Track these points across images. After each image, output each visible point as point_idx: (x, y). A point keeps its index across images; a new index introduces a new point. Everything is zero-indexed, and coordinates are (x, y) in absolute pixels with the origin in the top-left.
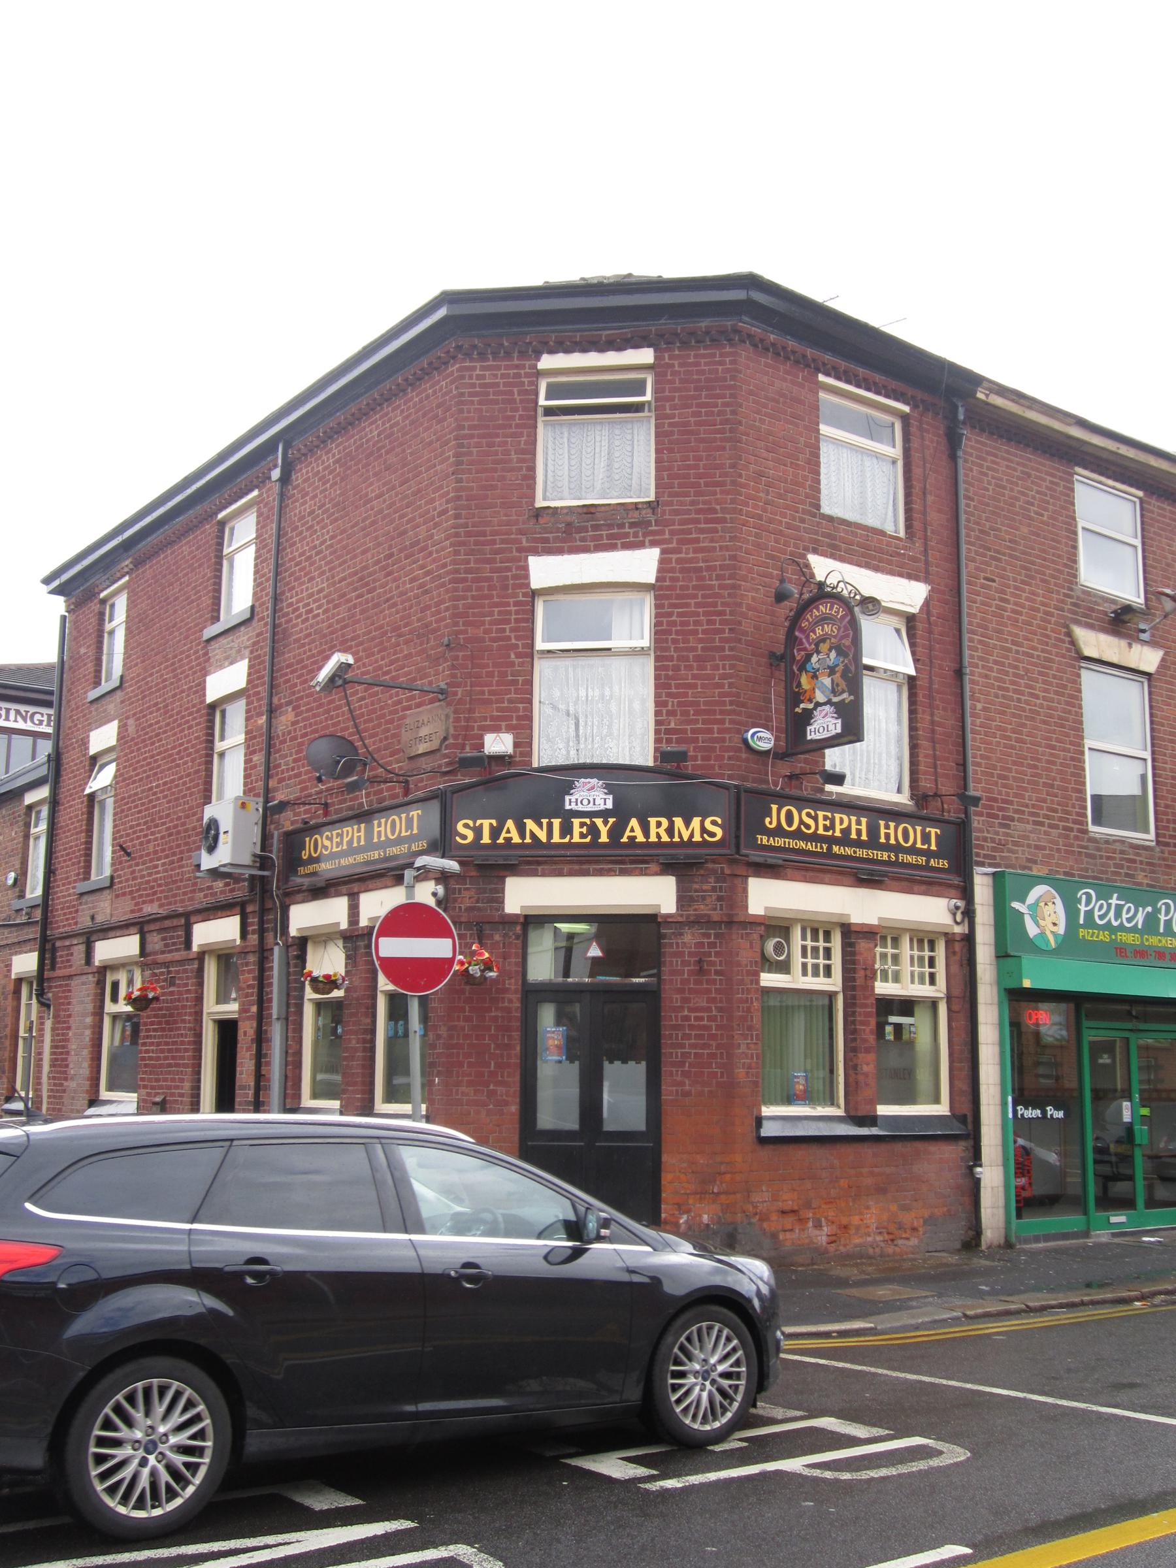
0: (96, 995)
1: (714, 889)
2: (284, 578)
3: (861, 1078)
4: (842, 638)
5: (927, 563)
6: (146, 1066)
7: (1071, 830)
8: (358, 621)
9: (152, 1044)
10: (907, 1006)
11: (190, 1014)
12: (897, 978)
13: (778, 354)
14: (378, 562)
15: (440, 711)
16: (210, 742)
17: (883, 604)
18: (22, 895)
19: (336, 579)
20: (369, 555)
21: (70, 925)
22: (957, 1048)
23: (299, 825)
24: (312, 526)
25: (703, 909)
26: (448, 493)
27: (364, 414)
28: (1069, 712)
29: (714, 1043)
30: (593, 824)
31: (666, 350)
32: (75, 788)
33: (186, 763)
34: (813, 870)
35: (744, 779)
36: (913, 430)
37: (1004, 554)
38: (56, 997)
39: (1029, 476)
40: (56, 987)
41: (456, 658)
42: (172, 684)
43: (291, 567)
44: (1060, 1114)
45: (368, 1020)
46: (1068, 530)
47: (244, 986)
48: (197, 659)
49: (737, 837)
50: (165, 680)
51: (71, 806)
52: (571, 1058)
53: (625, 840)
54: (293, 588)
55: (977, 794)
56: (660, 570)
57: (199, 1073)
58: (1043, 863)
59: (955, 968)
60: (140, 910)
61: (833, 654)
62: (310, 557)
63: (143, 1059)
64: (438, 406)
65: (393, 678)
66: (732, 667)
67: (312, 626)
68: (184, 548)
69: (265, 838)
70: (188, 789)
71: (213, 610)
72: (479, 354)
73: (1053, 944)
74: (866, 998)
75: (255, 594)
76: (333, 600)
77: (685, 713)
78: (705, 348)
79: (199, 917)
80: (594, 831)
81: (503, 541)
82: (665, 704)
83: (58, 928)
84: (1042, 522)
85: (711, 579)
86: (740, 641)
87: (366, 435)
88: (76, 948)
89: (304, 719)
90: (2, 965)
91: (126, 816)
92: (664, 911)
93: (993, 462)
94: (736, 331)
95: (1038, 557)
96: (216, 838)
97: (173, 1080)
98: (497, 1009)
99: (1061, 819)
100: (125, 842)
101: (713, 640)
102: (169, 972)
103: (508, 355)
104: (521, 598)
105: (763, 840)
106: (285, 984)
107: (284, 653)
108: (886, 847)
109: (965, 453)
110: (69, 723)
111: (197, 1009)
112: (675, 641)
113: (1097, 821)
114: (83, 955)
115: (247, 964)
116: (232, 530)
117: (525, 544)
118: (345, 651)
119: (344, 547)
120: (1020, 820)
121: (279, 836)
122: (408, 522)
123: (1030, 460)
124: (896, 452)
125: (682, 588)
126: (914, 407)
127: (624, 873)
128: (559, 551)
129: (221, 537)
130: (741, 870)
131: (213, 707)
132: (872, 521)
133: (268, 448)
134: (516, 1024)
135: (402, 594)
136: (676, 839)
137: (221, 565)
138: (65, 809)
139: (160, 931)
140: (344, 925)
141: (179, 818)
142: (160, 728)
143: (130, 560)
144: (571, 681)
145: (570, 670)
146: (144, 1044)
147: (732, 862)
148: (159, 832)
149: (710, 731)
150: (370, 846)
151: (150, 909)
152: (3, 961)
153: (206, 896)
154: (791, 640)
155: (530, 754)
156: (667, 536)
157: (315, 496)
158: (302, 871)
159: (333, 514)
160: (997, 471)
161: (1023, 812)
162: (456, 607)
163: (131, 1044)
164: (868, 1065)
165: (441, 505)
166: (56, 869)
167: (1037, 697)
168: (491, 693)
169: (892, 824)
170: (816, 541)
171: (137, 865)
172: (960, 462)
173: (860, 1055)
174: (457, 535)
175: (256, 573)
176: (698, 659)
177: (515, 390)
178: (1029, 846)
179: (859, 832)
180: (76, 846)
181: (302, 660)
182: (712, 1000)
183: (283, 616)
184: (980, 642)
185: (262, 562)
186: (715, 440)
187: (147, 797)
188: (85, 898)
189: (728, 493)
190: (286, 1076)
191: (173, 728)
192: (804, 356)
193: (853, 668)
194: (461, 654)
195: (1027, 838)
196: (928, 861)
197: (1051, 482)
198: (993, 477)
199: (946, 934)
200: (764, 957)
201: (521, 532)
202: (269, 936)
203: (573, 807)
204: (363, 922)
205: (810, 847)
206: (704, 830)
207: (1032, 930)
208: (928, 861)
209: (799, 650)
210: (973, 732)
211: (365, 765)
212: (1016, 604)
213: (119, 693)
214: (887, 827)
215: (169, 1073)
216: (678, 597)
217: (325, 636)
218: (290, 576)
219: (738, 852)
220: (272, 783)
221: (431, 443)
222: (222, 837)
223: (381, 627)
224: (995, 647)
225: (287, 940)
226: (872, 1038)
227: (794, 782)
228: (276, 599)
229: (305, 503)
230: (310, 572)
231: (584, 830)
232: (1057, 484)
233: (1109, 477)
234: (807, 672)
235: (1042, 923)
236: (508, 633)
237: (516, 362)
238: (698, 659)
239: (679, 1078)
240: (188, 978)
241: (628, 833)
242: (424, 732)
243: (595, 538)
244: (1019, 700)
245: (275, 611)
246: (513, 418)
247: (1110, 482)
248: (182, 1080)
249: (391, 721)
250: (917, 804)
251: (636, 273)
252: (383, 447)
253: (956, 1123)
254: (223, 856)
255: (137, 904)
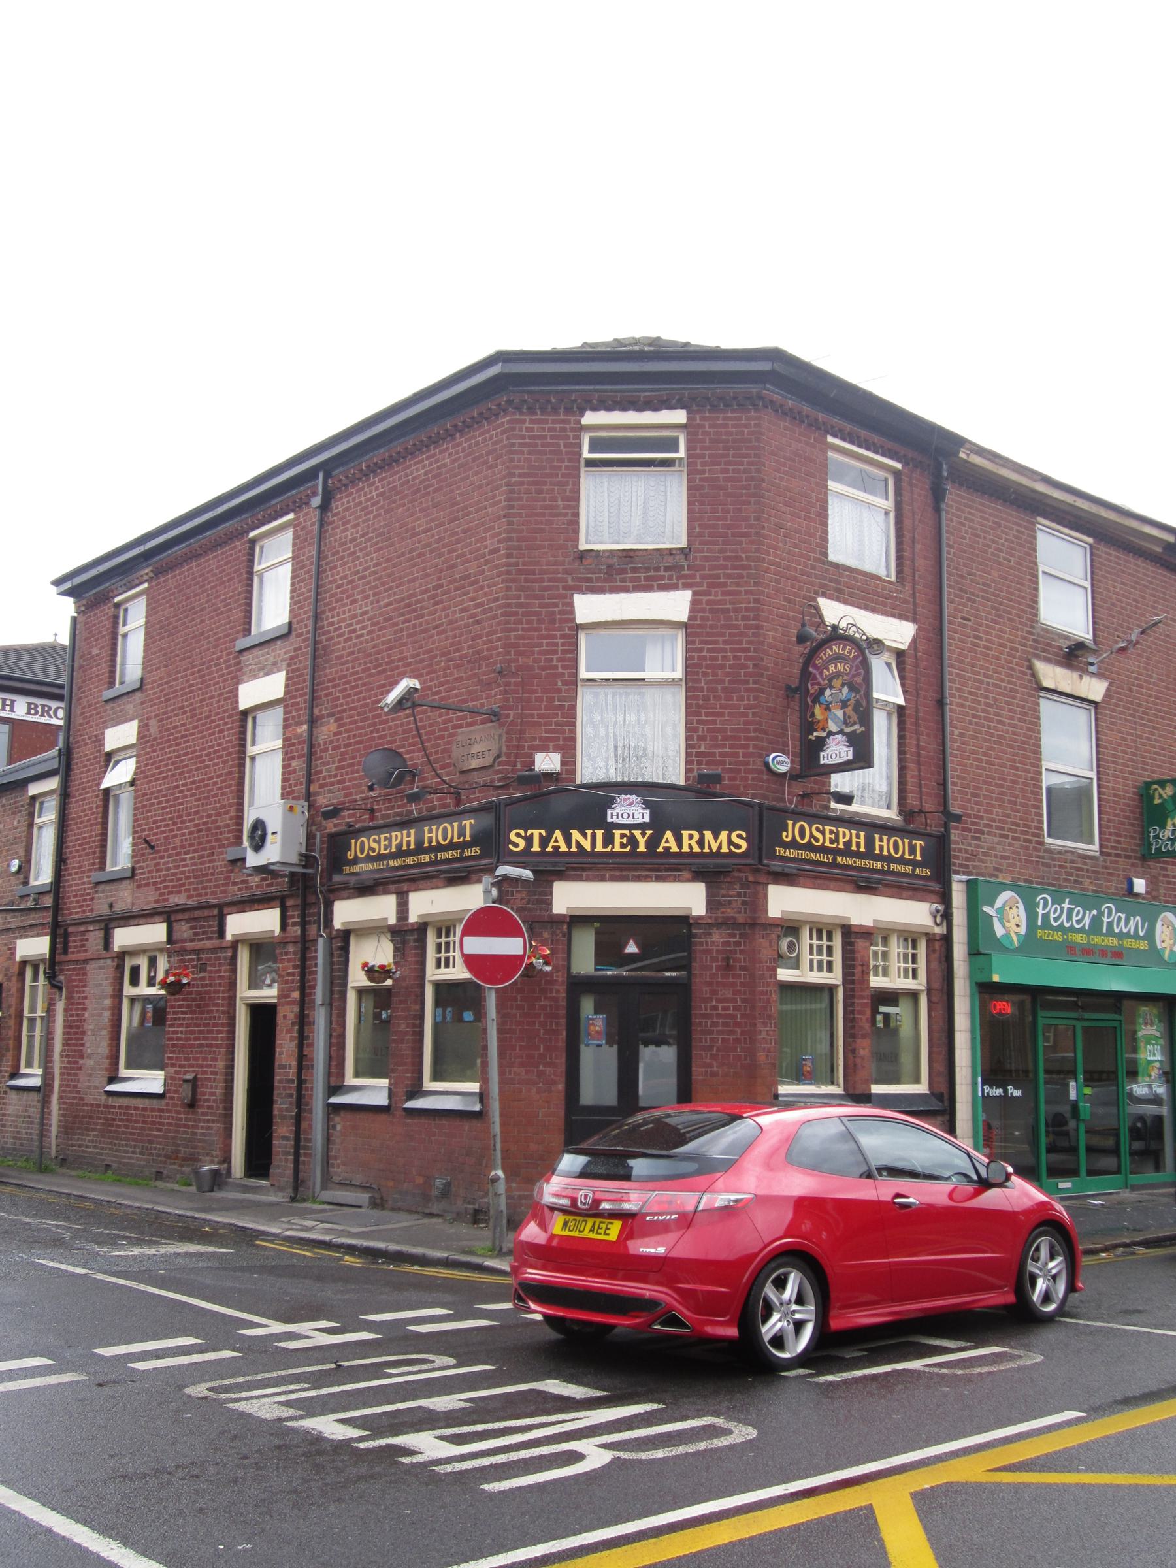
0: (115, 978)
1: (739, 895)
2: (325, 598)
3: (858, 1061)
4: (854, 676)
5: (915, 604)
6: (173, 1045)
7: (1030, 841)
8: (405, 644)
9: (180, 1025)
10: (890, 997)
11: (224, 998)
12: (886, 974)
13: (795, 418)
14: (427, 591)
15: (493, 731)
16: (243, 746)
17: (887, 643)
18: (26, 882)
19: (382, 603)
20: (417, 584)
21: (84, 912)
22: (935, 1034)
23: (343, 828)
24: (354, 553)
25: (729, 912)
26: (499, 534)
27: (409, 453)
28: (1030, 737)
29: (739, 1030)
30: (633, 835)
31: (698, 412)
32: (88, 782)
33: (215, 765)
34: (821, 878)
35: (765, 797)
36: (904, 485)
37: (978, 596)
38: (69, 980)
39: (999, 525)
40: (68, 970)
41: (508, 684)
42: (199, 689)
43: (331, 589)
44: (1018, 1093)
45: (418, 1007)
46: (1031, 574)
47: (284, 973)
48: (227, 667)
49: (760, 849)
50: (192, 685)
51: (84, 799)
52: (610, 1043)
53: (660, 850)
54: (335, 608)
55: (959, 812)
56: (692, 611)
57: (233, 1053)
58: (1007, 871)
59: (934, 965)
60: (167, 900)
61: (845, 690)
62: (353, 581)
63: (170, 1039)
64: (488, 453)
65: (442, 699)
66: (755, 698)
67: (355, 645)
68: (212, 562)
69: (310, 837)
70: (219, 789)
71: (245, 623)
72: (529, 408)
73: (1016, 943)
74: (863, 990)
75: (291, 611)
76: (378, 623)
77: (714, 739)
78: (733, 411)
79: (234, 909)
80: (633, 841)
81: (550, 580)
82: (695, 730)
83: (71, 914)
84: (1010, 567)
85: (737, 620)
86: (762, 675)
87: (412, 473)
88: (92, 934)
89: (347, 731)
90: (5, 948)
91: (149, 811)
92: (695, 913)
93: (970, 513)
94: (760, 397)
95: (1006, 598)
96: (263, 838)
97: (205, 1059)
98: (546, 998)
99: (1022, 832)
100: (148, 835)
101: (739, 674)
102: (199, 959)
103: (555, 410)
104: (567, 632)
105: (781, 851)
106: (328, 970)
107: (325, 669)
108: (880, 858)
109: (948, 505)
110: (80, 720)
111: (231, 993)
112: (704, 674)
113: (1049, 836)
114: (102, 942)
115: (286, 954)
116: (262, 548)
117: (570, 583)
118: (415, 677)
119: (390, 575)
120: (989, 833)
121: (322, 836)
122: (458, 557)
123: (1000, 511)
124: (890, 504)
125: (711, 627)
126: (905, 464)
127: (659, 879)
128: (601, 590)
129: (252, 554)
130: (762, 878)
131: (245, 713)
132: (868, 567)
133: (311, 474)
134: (563, 1012)
135: (451, 623)
136: (706, 850)
137: (252, 580)
138: (77, 801)
139: (188, 920)
140: (392, 920)
141: (209, 816)
142: (186, 730)
143: (150, 568)
144: (611, 707)
145: (610, 697)
146: (172, 1026)
147: (756, 871)
148: (187, 828)
149: (737, 755)
150: (420, 849)
151: (176, 900)
152: (5, 944)
153: (240, 889)
154: (805, 675)
155: (574, 772)
156: (698, 580)
157: (358, 525)
158: (346, 869)
159: (377, 543)
160: (972, 521)
161: (991, 826)
162: (508, 638)
163: (154, 1023)
164: (864, 1049)
165: (492, 544)
166: (67, 858)
167: (1003, 724)
168: (540, 716)
169: (885, 838)
170: (824, 586)
171: (162, 857)
172: (944, 514)
173: (859, 1041)
174: (508, 572)
175: (292, 591)
176: (725, 690)
177: (562, 442)
178: (996, 856)
179: (858, 844)
180: (91, 837)
181: (345, 676)
182: (736, 992)
183: (324, 634)
184: (958, 675)
185: (299, 582)
186: (741, 495)
187: (173, 794)
188: (102, 887)
189: (752, 542)
190: (330, 1057)
191: (202, 732)
192: (816, 420)
193: (864, 704)
194: (513, 680)
195: (994, 849)
196: (914, 870)
197: (1018, 531)
198: (970, 527)
199: (927, 934)
200: (780, 956)
201: (566, 572)
202: (312, 930)
203: (615, 820)
204: (413, 918)
205: (819, 857)
206: (730, 842)
207: (999, 931)
208: (914, 870)
209: (813, 684)
210: (952, 755)
211: (414, 776)
212: (987, 640)
213: (138, 694)
214: (881, 840)
215: (201, 1052)
216: (708, 634)
217: (369, 655)
218: (331, 597)
219: (760, 861)
220: (314, 788)
221: (480, 487)
222: (269, 838)
223: (431, 651)
224: (970, 679)
225: (331, 933)
226: (867, 1026)
227: (806, 800)
228: (317, 617)
229: (347, 530)
230: (353, 595)
231: (624, 840)
232: (1022, 533)
233: (1065, 526)
234: (820, 704)
235: (1007, 924)
236: (555, 663)
237: (562, 417)
238: (725, 690)
239: (708, 1061)
240: (220, 965)
241: (663, 844)
242: (476, 749)
243: (633, 580)
244: (989, 727)
245: (315, 629)
246: (559, 468)
247: (1066, 530)
248: (215, 1060)
249: (442, 737)
250: (905, 820)
251: (664, 337)
252: (430, 486)
253: (934, 1101)
254: (272, 853)
255: (162, 895)
